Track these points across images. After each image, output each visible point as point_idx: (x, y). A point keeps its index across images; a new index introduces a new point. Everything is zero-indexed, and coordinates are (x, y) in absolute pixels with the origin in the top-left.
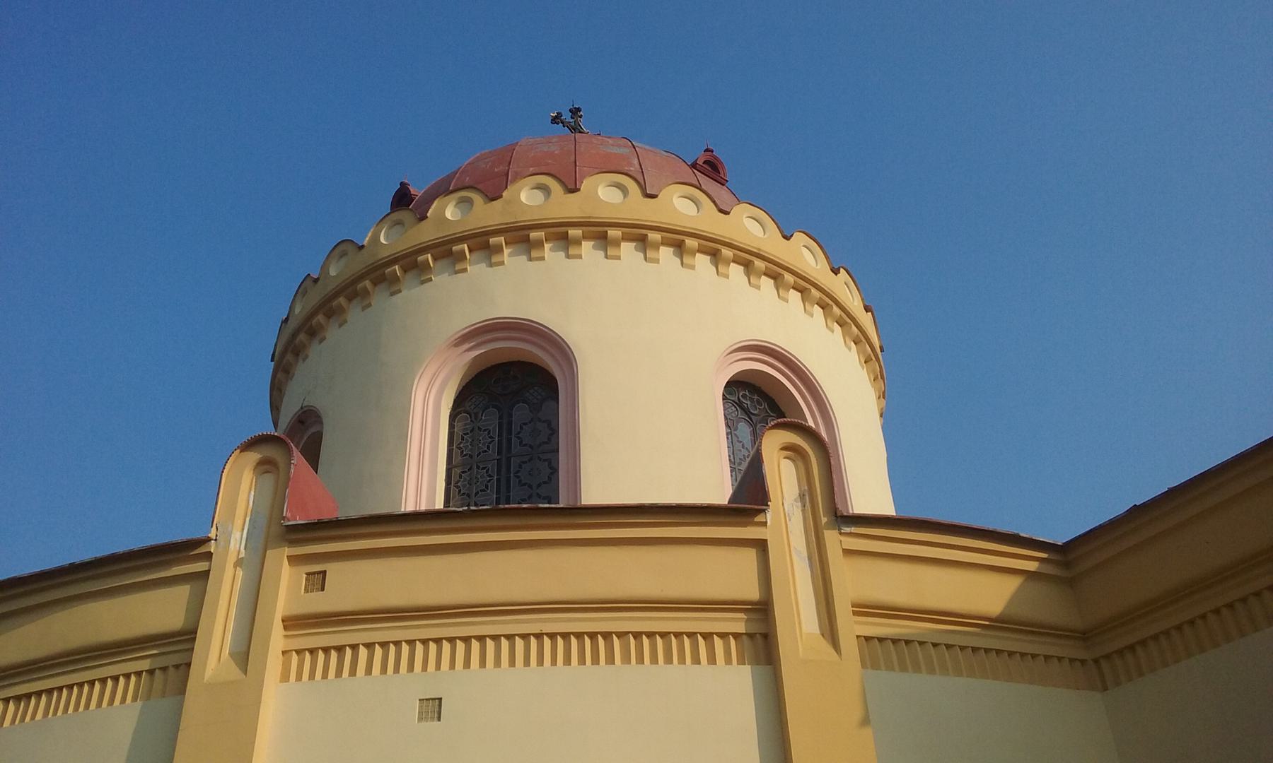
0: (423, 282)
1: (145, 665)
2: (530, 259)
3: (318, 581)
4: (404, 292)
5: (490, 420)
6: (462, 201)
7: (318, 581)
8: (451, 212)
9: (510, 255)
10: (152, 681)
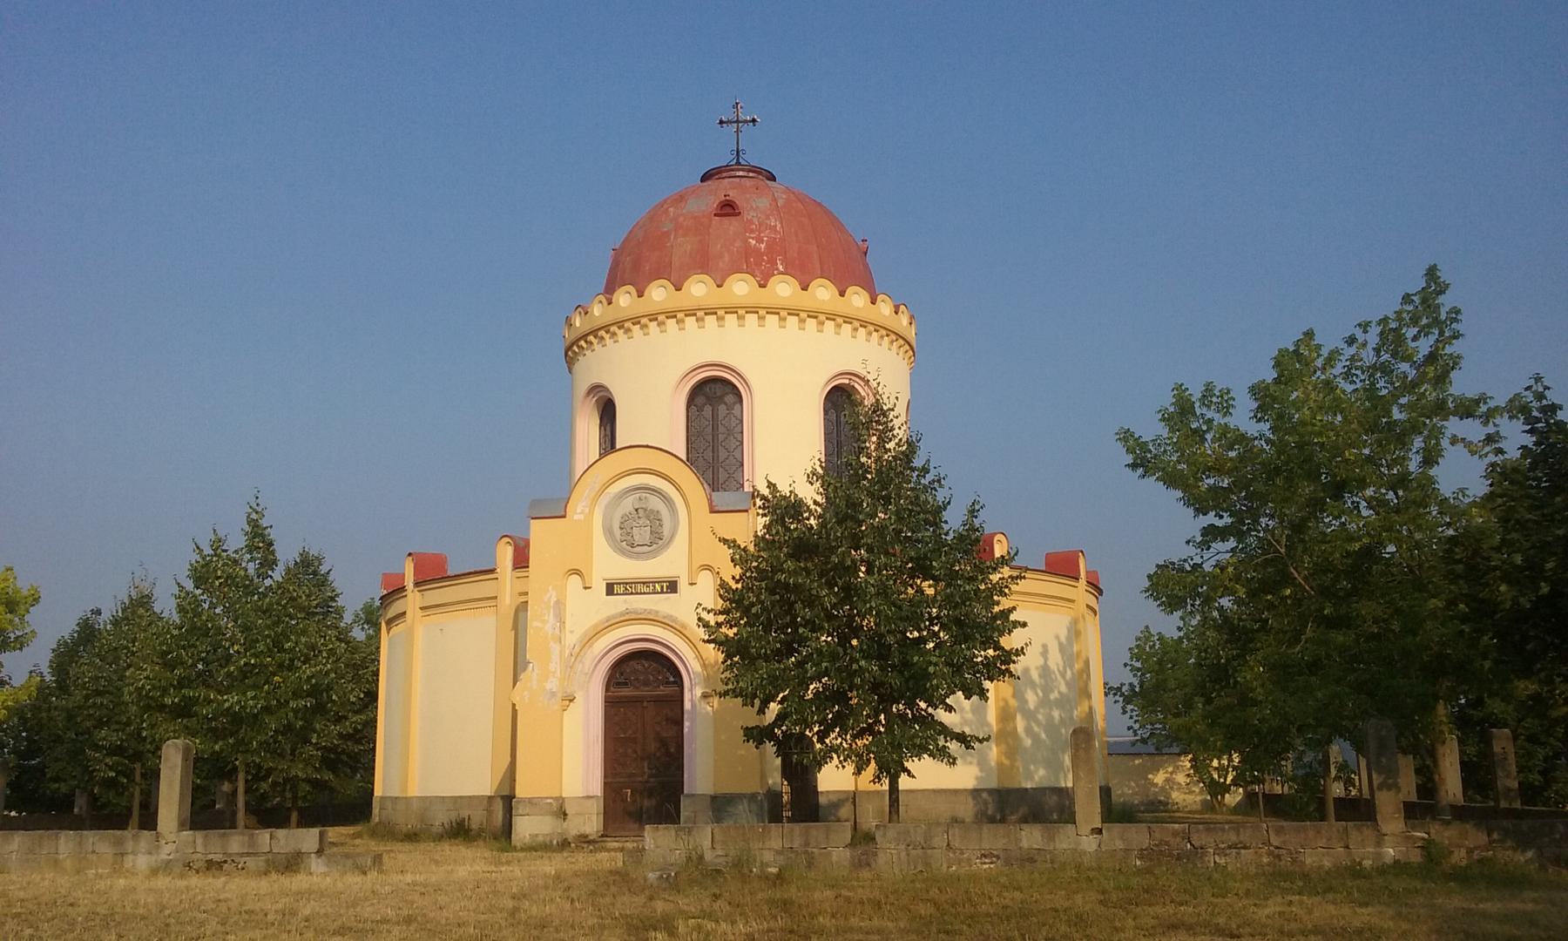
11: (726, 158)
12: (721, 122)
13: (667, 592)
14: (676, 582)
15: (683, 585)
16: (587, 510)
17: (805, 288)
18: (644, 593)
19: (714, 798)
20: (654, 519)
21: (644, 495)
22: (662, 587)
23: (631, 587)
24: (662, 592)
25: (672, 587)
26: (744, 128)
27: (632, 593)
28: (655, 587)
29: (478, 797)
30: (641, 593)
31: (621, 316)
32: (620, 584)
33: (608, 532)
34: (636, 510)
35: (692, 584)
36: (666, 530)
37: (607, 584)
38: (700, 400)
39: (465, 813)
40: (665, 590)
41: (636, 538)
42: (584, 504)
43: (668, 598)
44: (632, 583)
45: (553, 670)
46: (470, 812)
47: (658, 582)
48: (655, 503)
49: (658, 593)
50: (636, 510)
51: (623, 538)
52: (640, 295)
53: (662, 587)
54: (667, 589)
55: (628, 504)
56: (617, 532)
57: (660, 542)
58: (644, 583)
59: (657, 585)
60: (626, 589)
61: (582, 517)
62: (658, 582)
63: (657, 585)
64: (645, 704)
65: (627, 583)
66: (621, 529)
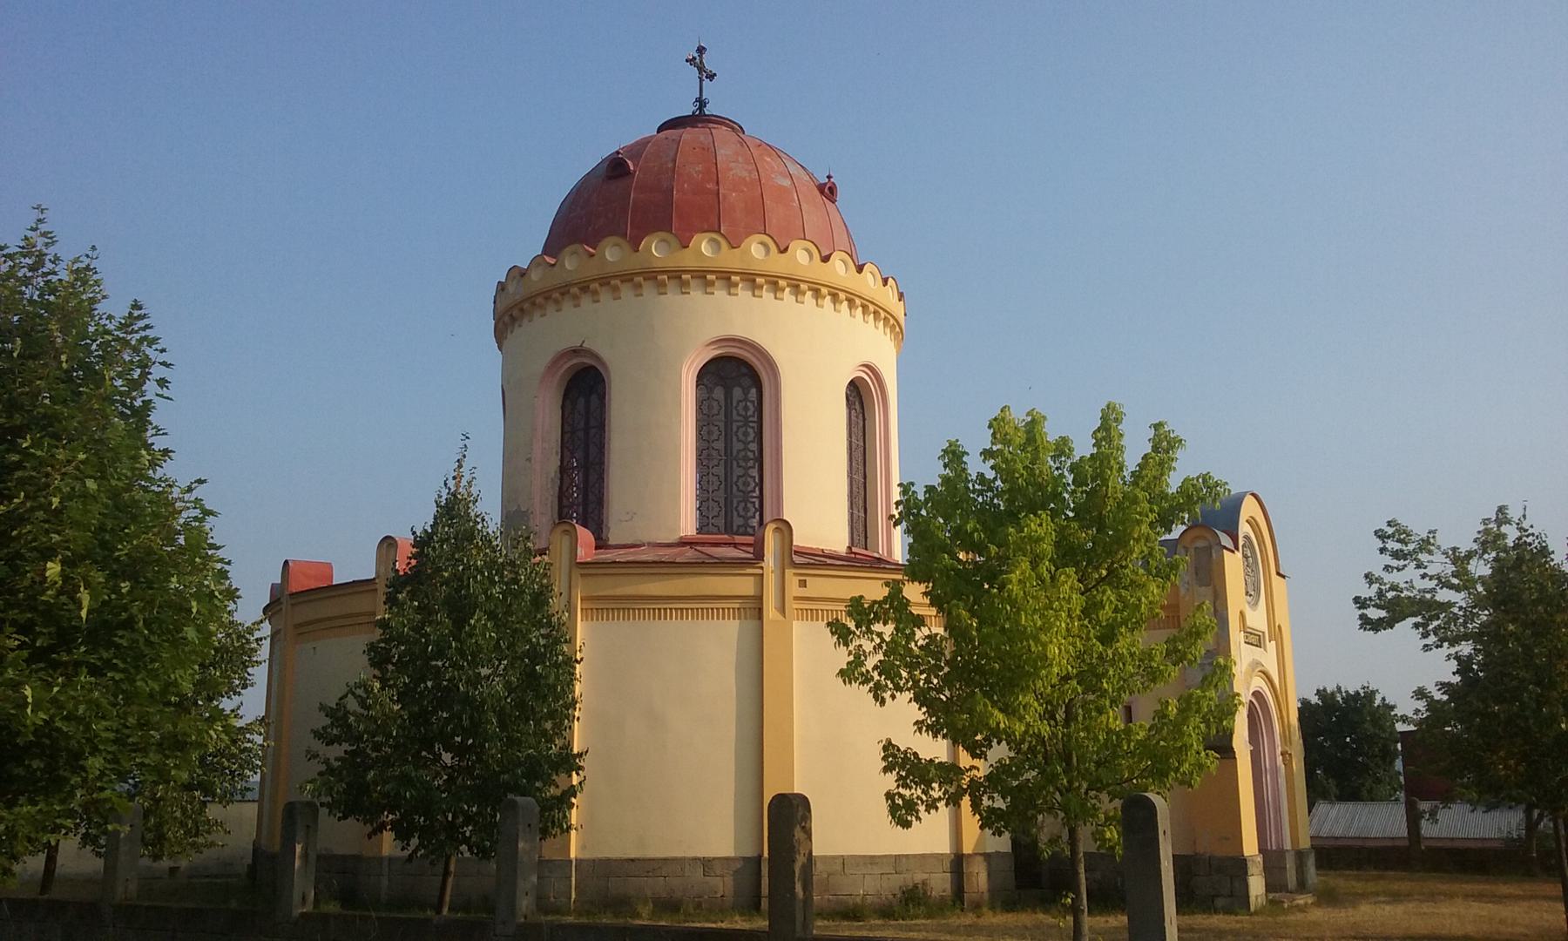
0: (683, 293)
1: (737, 606)
2: (754, 296)
3: (803, 584)
4: (669, 295)
5: (719, 393)
6: (712, 240)
7: (803, 584)
8: (705, 248)
9: (742, 288)
10: (745, 613)
11: (688, 109)
29: (932, 856)
39: (919, 877)
46: (925, 876)
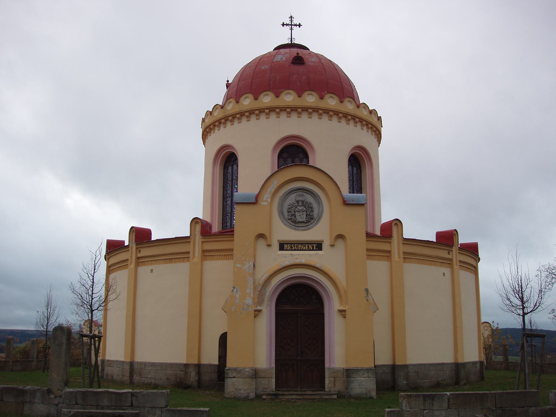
11: (287, 42)
12: (283, 25)
13: (316, 250)
14: (321, 244)
15: (325, 246)
16: (269, 200)
17: (342, 102)
18: (303, 250)
19: (348, 371)
20: (309, 208)
21: (302, 193)
22: (313, 247)
23: (295, 247)
24: (313, 250)
25: (319, 246)
26: (293, 27)
27: (295, 250)
28: (308, 246)
30: (300, 250)
31: (244, 109)
32: (288, 244)
33: (281, 213)
34: (298, 202)
35: (332, 246)
36: (315, 214)
37: (280, 243)
38: (285, 155)
40: (315, 249)
41: (298, 218)
42: (267, 196)
43: (317, 254)
44: (295, 244)
45: (249, 292)
47: (310, 244)
48: (309, 199)
49: (311, 250)
50: (298, 202)
51: (290, 217)
52: (256, 99)
53: (313, 247)
54: (316, 248)
55: (292, 199)
56: (286, 214)
57: (312, 221)
58: (302, 244)
59: (310, 245)
60: (291, 247)
61: (266, 203)
62: (310, 244)
63: (310, 245)
64: (299, 315)
65: (292, 244)
66: (289, 212)
